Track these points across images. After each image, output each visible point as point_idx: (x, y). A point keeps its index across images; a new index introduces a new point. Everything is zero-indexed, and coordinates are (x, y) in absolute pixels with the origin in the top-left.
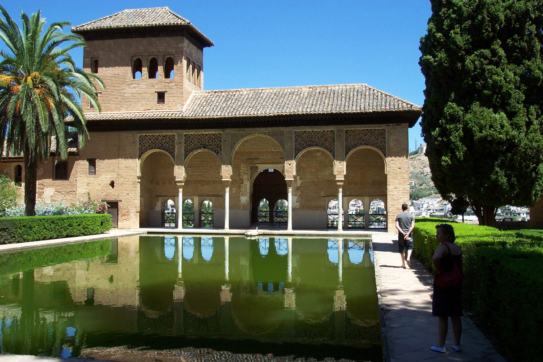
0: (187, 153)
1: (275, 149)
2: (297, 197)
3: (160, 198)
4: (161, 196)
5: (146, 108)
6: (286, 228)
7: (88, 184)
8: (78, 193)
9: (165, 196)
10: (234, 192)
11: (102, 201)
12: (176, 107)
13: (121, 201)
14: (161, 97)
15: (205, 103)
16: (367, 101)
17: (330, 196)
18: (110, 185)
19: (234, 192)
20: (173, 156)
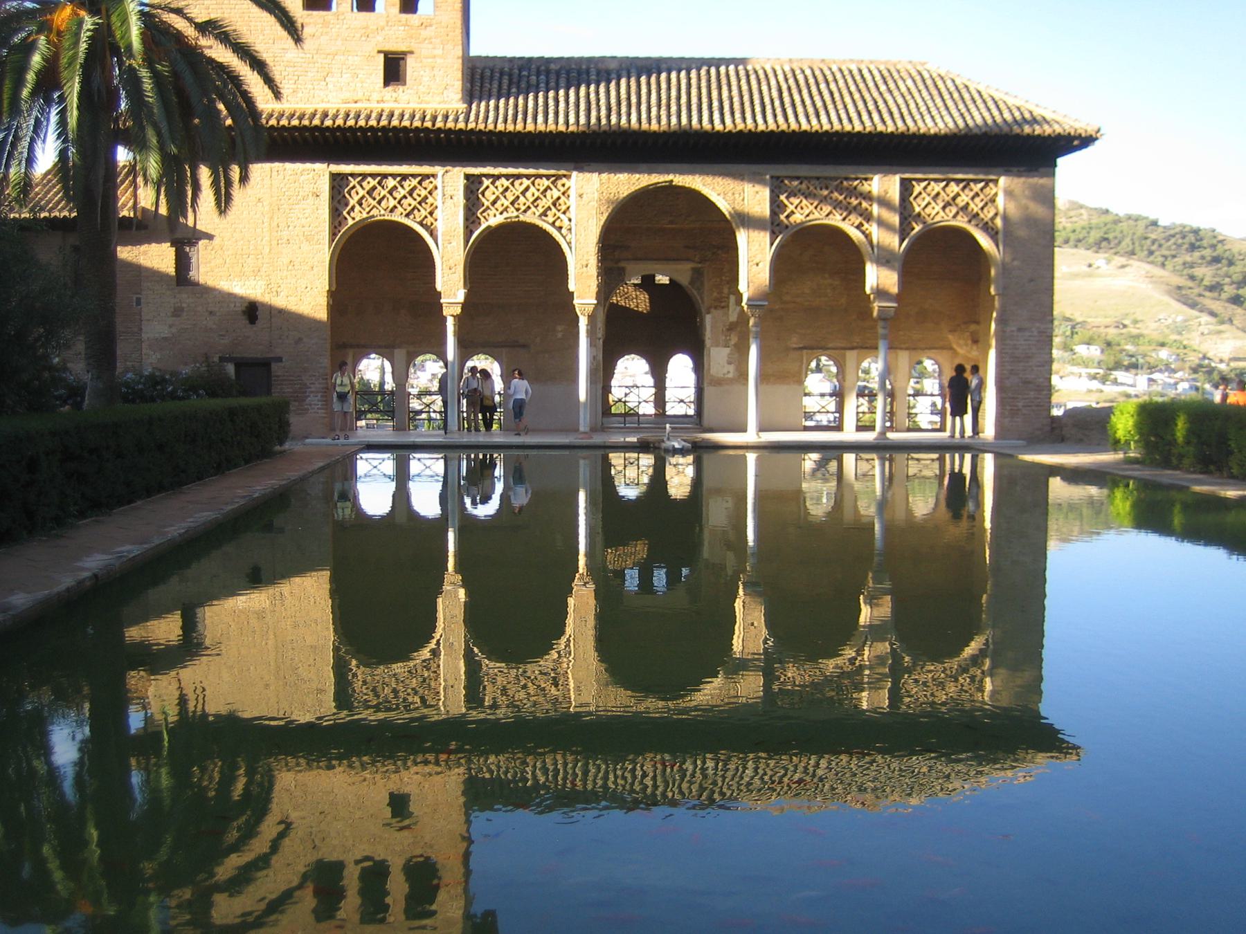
0: (471, 226)
1: (671, 222)
2: (727, 350)
3: (351, 352)
4: (352, 346)
5: (347, 95)
6: (743, 429)
7: (177, 312)
8: (145, 336)
9: (364, 346)
10: (560, 335)
11: (222, 359)
12: (438, 99)
13: (279, 359)
14: (394, 69)
15: (514, 90)
16: (950, 103)
17: (812, 348)
18: (244, 312)
19: (560, 335)
20: (432, 233)
